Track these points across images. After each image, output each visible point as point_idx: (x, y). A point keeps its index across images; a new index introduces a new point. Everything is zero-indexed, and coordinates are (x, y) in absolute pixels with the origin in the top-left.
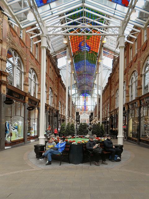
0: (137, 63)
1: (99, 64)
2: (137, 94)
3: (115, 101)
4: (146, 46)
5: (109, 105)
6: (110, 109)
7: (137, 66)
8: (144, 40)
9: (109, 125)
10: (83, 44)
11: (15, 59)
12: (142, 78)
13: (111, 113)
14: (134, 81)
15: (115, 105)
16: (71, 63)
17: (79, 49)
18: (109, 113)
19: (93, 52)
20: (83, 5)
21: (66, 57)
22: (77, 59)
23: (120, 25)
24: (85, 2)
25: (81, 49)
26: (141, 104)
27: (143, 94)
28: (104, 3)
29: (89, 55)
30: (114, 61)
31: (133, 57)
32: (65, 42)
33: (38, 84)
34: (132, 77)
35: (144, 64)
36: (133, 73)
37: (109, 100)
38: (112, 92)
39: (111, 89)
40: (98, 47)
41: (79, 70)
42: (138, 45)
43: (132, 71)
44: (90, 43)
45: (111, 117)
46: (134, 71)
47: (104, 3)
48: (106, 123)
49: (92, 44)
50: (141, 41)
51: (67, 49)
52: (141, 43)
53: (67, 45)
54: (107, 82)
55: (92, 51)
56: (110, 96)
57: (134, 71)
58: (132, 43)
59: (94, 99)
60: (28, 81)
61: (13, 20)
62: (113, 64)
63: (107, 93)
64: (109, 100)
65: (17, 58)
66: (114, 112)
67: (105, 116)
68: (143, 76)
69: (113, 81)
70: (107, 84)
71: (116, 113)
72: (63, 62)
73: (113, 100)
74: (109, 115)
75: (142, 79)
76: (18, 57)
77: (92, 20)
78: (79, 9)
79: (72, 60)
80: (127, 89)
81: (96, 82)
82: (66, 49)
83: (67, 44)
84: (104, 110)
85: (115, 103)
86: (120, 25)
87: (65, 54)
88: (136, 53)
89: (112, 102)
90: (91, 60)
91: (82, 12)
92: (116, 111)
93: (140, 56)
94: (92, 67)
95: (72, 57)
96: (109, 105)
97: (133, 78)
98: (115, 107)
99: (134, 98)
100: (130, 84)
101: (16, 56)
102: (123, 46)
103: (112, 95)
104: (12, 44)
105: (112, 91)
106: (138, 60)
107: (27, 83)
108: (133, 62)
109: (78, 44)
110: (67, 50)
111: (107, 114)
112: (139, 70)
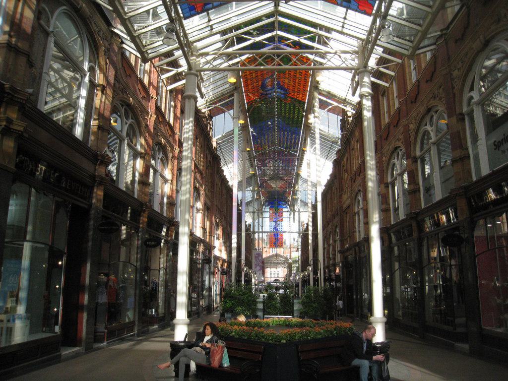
0: (401, 129)
1: (308, 127)
3: (354, 222)
4: (418, 94)
5: (338, 231)
6: (342, 245)
7: (401, 137)
8: (411, 79)
11: (126, 124)
14: (399, 171)
16: (244, 128)
17: (262, 94)
18: (341, 252)
20: (276, 13)
21: (231, 112)
22: (255, 116)
23: (357, 49)
24: (280, 5)
25: (267, 94)
28: (319, 6)
31: (389, 115)
32: (233, 80)
34: (392, 161)
36: (393, 153)
37: (337, 219)
38: (345, 197)
39: (341, 189)
41: (261, 142)
42: (399, 89)
43: (391, 148)
45: (346, 265)
46: (396, 148)
47: (319, 6)
48: (333, 280)
50: (404, 82)
51: (235, 95)
52: (405, 84)
53: (236, 87)
57: (396, 148)
58: (387, 85)
59: (299, 214)
61: (133, 45)
64: (337, 219)
65: (130, 121)
67: (328, 262)
68: (419, 161)
69: (346, 171)
70: (331, 176)
71: (358, 254)
72: (224, 125)
74: (338, 257)
76: (132, 119)
77: (296, 38)
78: (268, 16)
79: (246, 120)
80: (384, 191)
82: (233, 95)
83: (235, 83)
84: (326, 246)
85: (354, 227)
86: (357, 49)
87: (229, 106)
90: (289, 118)
91: (273, 23)
92: (357, 249)
93: (407, 114)
94: (292, 135)
95: (243, 111)
96: (338, 231)
97: (394, 164)
98: (354, 238)
99: (402, 216)
100: (389, 180)
101: (127, 118)
102: (369, 93)
103: (345, 206)
104: (122, 92)
106: (403, 122)
108: (392, 127)
109: (260, 83)
110: (236, 97)
111: (334, 255)
112: (408, 145)
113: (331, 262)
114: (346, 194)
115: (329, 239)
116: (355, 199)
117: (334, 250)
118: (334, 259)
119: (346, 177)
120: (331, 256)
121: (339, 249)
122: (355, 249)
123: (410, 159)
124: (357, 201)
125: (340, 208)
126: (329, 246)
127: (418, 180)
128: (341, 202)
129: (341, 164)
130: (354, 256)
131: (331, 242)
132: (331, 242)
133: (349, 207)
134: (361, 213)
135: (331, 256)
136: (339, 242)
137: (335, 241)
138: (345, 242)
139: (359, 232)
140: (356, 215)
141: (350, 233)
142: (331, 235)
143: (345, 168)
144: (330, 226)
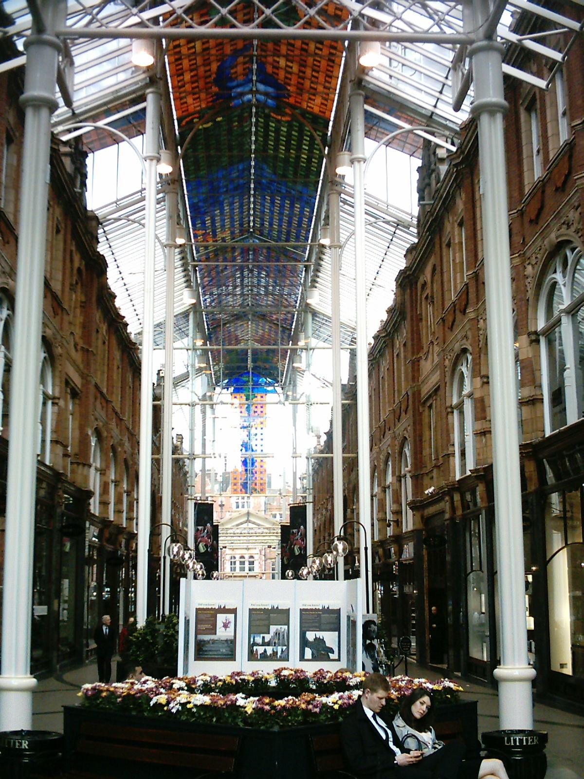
1: (334, 183)
5: (407, 451)
10: (240, 69)
18: (415, 506)
19: (304, 113)
29: (277, 131)
30: (426, 172)
38: (426, 366)
39: (416, 345)
40: (329, 89)
44: (282, 62)
49: (295, 68)
54: (386, 296)
55: (293, 107)
56: (417, 394)
62: (421, 191)
63: (391, 370)
66: (445, 505)
70: (390, 311)
73: (432, 417)
74: (409, 522)
81: (316, 300)
89: (431, 436)
92: (457, 497)
96: (407, 451)
103: (426, 390)
105: (422, 362)
111: (398, 513)
113: (390, 531)
114: (430, 356)
115: (385, 472)
118: (398, 523)
119: (430, 314)
120: (389, 516)
121: (410, 498)
122: (452, 499)
125: (414, 394)
126: (385, 492)
129: (416, 283)
130: (447, 516)
131: (390, 479)
132: (390, 479)
133: (437, 390)
135: (389, 516)
136: (409, 481)
137: (399, 478)
138: (426, 480)
139: (463, 454)
141: (437, 459)
142: (390, 463)
143: (428, 291)
144: (388, 440)
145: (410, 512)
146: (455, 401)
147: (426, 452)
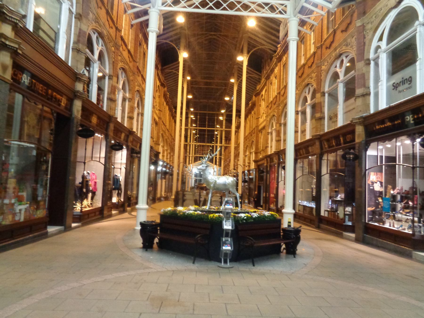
2: (313, 128)
9: (252, 186)
12: (325, 99)
13: (260, 163)
15: (267, 147)
18: (255, 161)
26: (322, 148)
27: (326, 130)
31: (305, 58)
33: (129, 99)
35: (327, 73)
60: (114, 93)
74: (253, 166)
75: (324, 102)
88: (312, 50)
103: (260, 127)
107: (112, 96)
116: (270, 122)
117: (249, 159)
121: (254, 159)
123: (320, 94)
124: (271, 124)
127: (324, 110)
128: (257, 123)
134: (274, 134)
140: (270, 134)
145: (253, 163)
146: (270, 131)
147: (259, 146)
